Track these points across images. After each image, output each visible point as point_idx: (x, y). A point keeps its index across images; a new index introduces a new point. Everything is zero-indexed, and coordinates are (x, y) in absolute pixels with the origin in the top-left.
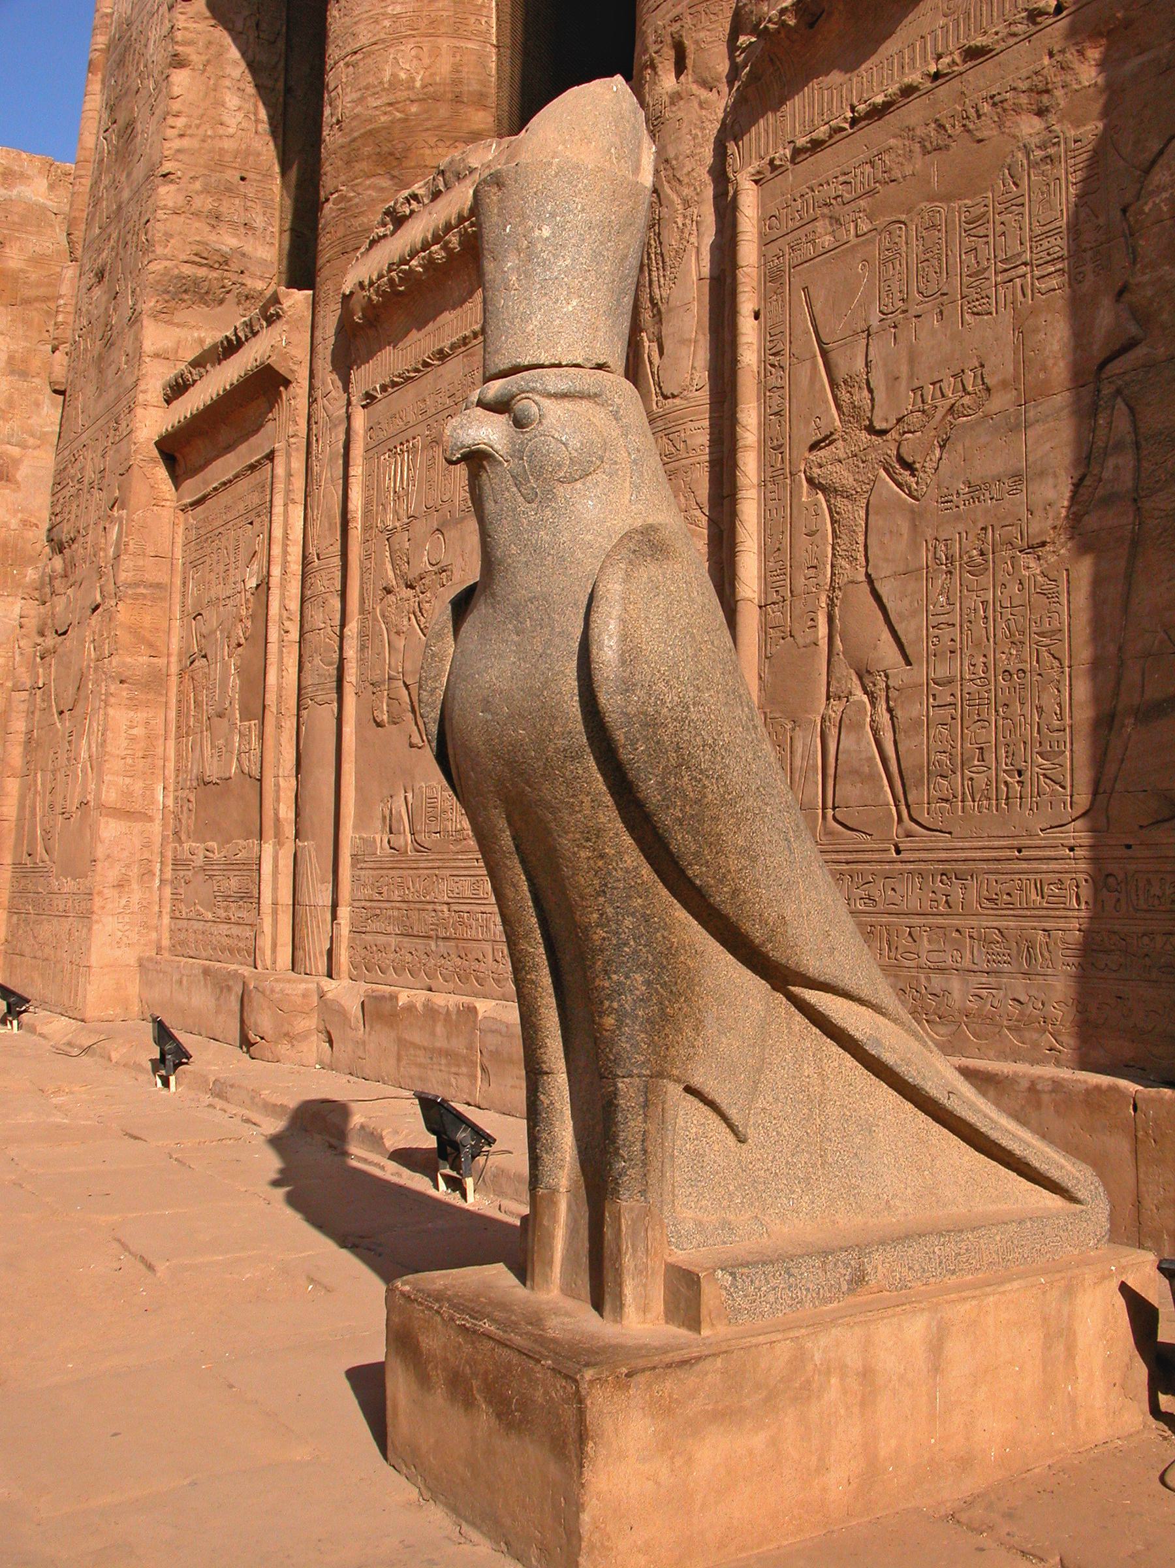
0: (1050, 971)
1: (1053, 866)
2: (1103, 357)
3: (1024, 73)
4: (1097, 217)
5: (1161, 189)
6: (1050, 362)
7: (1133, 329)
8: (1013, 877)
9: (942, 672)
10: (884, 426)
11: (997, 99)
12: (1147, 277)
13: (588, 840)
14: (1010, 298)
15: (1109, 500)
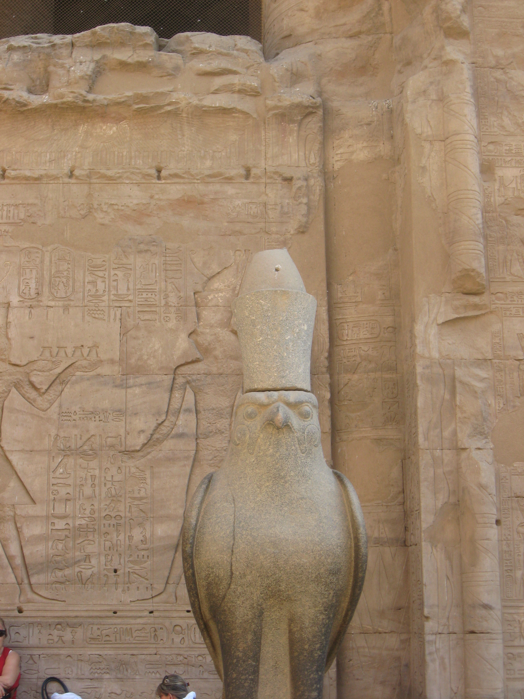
0: (137, 677)
1: (139, 621)
2: (179, 364)
3: (135, 202)
4: (179, 291)
5: (218, 291)
6: (145, 357)
7: (199, 356)
8: (111, 626)
9: (60, 509)
10: (18, 362)
11: (116, 207)
12: (208, 331)
13: (326, 611)
14: (118, 316)
15: (181, 436)
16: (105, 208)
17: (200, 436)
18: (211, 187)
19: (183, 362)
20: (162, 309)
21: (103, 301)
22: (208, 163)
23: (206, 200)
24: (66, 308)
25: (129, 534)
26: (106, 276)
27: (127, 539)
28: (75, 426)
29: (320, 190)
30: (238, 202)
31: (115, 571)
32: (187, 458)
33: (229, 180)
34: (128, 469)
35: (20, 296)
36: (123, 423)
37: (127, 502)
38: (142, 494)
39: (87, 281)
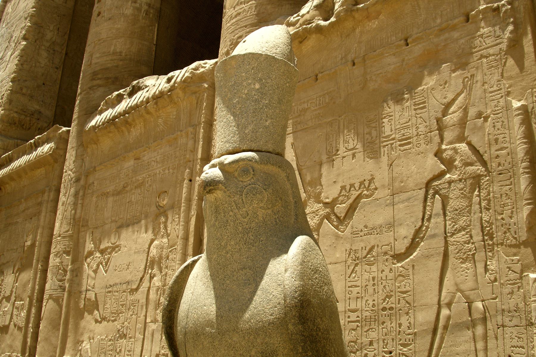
3: (393, 67)
4: (426, 122)
9: (353, 306)
10: (327, 200)
14: (386, 152)
15: (433, 236)
16: (374, 78)
17: (448, 235)
18: (442, 38)
19: (431, 176)
20: (415, 138)
21: (376, 144)
22: (439, 21)
23: (439, 48)
24: (354, 156)
25: (398, 322)
26: (377, 126)
27: (398, 325)
28: (362, 241)
29: (524, 8)
30: (463, 41)
31: (391, 353)
32: (438, 254)
33: (454, 28)
34: (396, 270)
35: (327, 155)
36: (392, 233)
37: (397, 295)
38: (408, 288)
39: (365, 132)
